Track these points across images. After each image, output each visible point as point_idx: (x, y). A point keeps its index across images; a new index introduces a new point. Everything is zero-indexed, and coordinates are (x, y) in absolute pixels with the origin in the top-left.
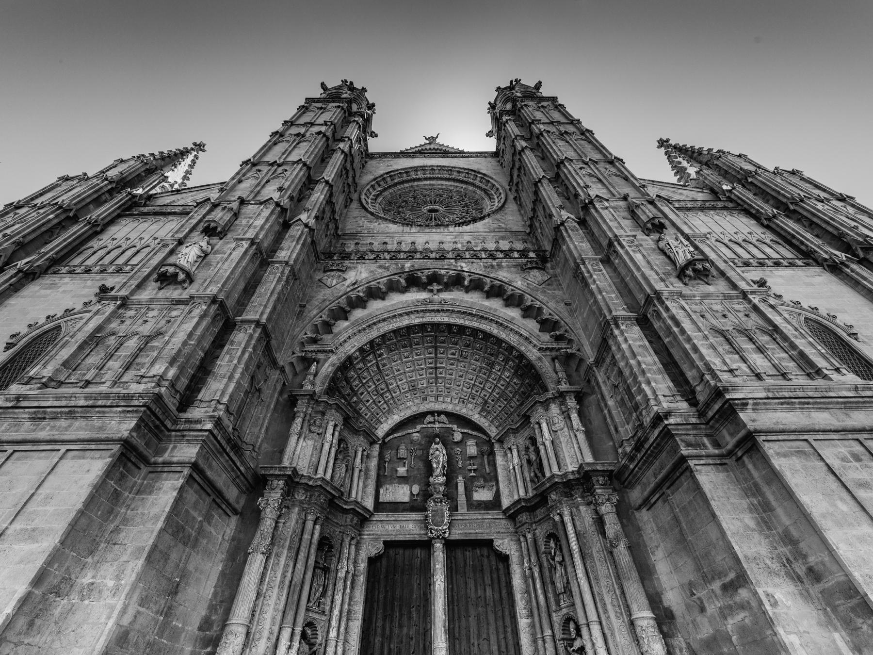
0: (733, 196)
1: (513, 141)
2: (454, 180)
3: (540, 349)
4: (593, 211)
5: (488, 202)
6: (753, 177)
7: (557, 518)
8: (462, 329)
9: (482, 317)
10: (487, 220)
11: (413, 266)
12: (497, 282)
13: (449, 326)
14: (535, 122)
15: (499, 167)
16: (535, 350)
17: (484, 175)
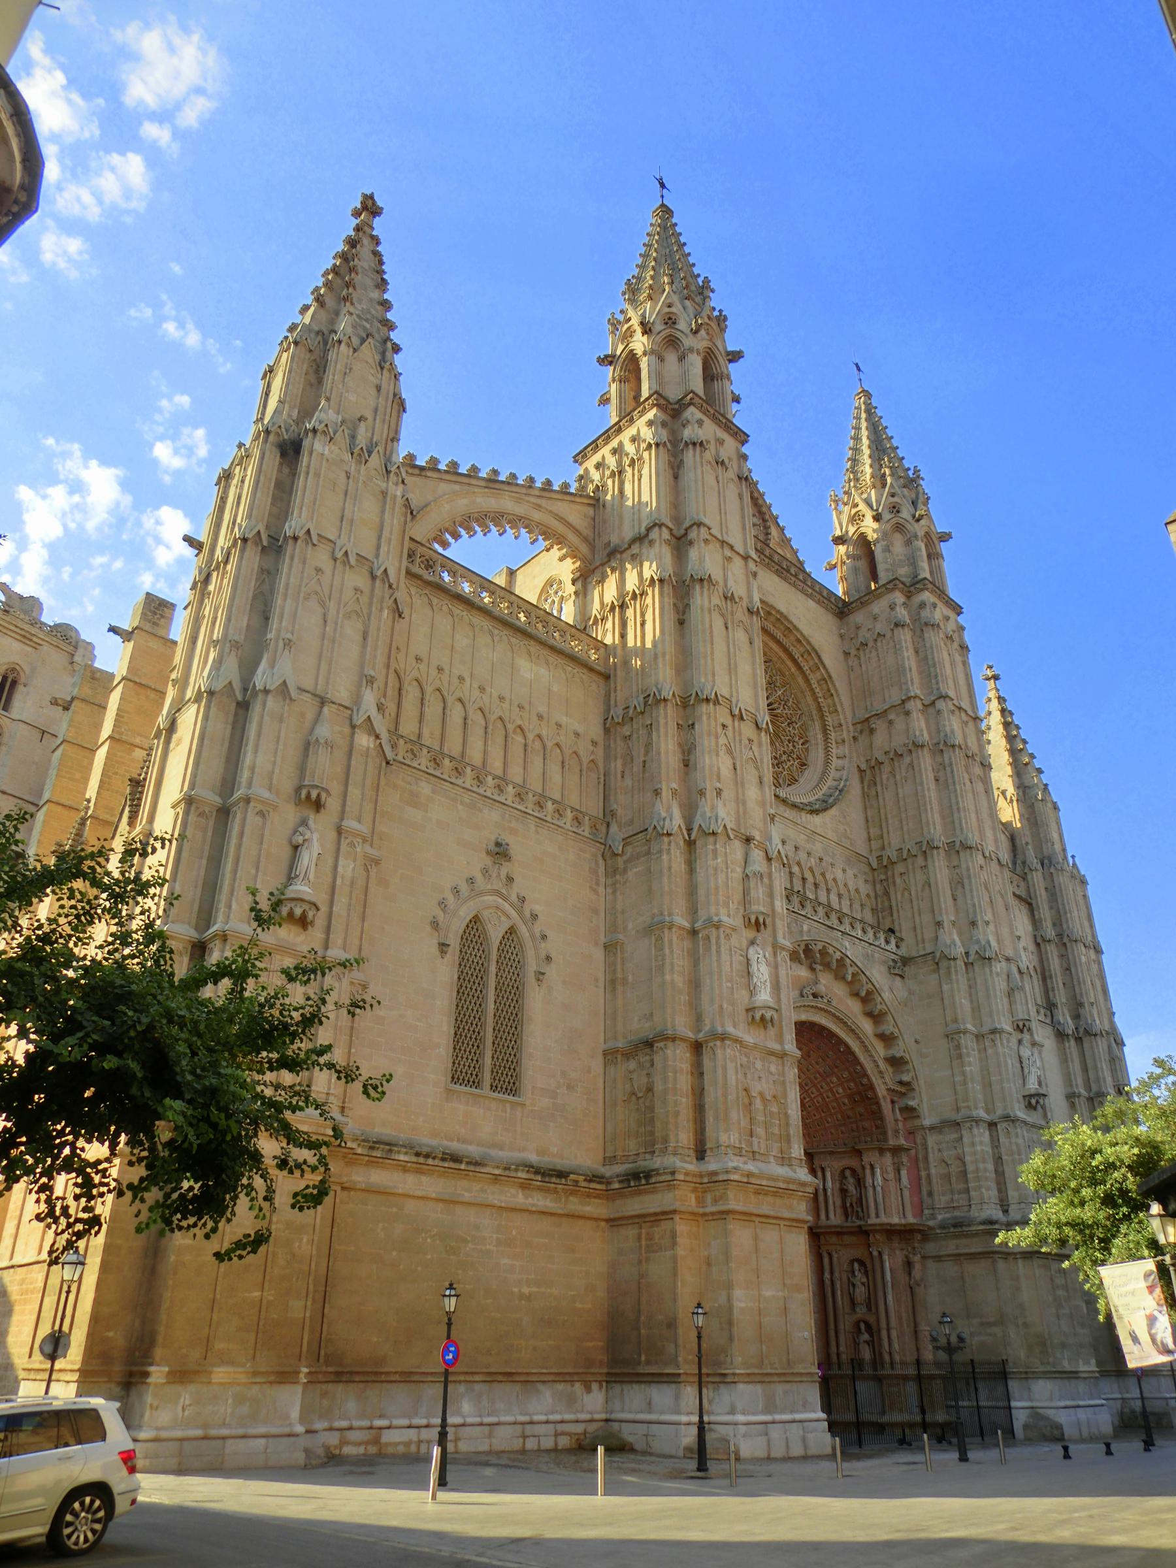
0: (1029, 877)
1: (909, 698)
2: (786, 650)
3: (889, 1090)
4: (987, 970)
5: (820, 736)
6: (1056, 869)
7: (875, 1253)
8: (831, 1034)
9: (853, 1031)
10: (833, 812)
11: (809, 931)
12: (870, 986)
13: (823, 1028)
14: (950, 703)
15: (841, 657)
16: (883, 1087)
17: (830, 677)
